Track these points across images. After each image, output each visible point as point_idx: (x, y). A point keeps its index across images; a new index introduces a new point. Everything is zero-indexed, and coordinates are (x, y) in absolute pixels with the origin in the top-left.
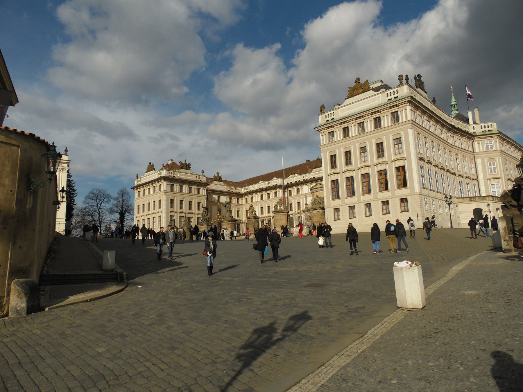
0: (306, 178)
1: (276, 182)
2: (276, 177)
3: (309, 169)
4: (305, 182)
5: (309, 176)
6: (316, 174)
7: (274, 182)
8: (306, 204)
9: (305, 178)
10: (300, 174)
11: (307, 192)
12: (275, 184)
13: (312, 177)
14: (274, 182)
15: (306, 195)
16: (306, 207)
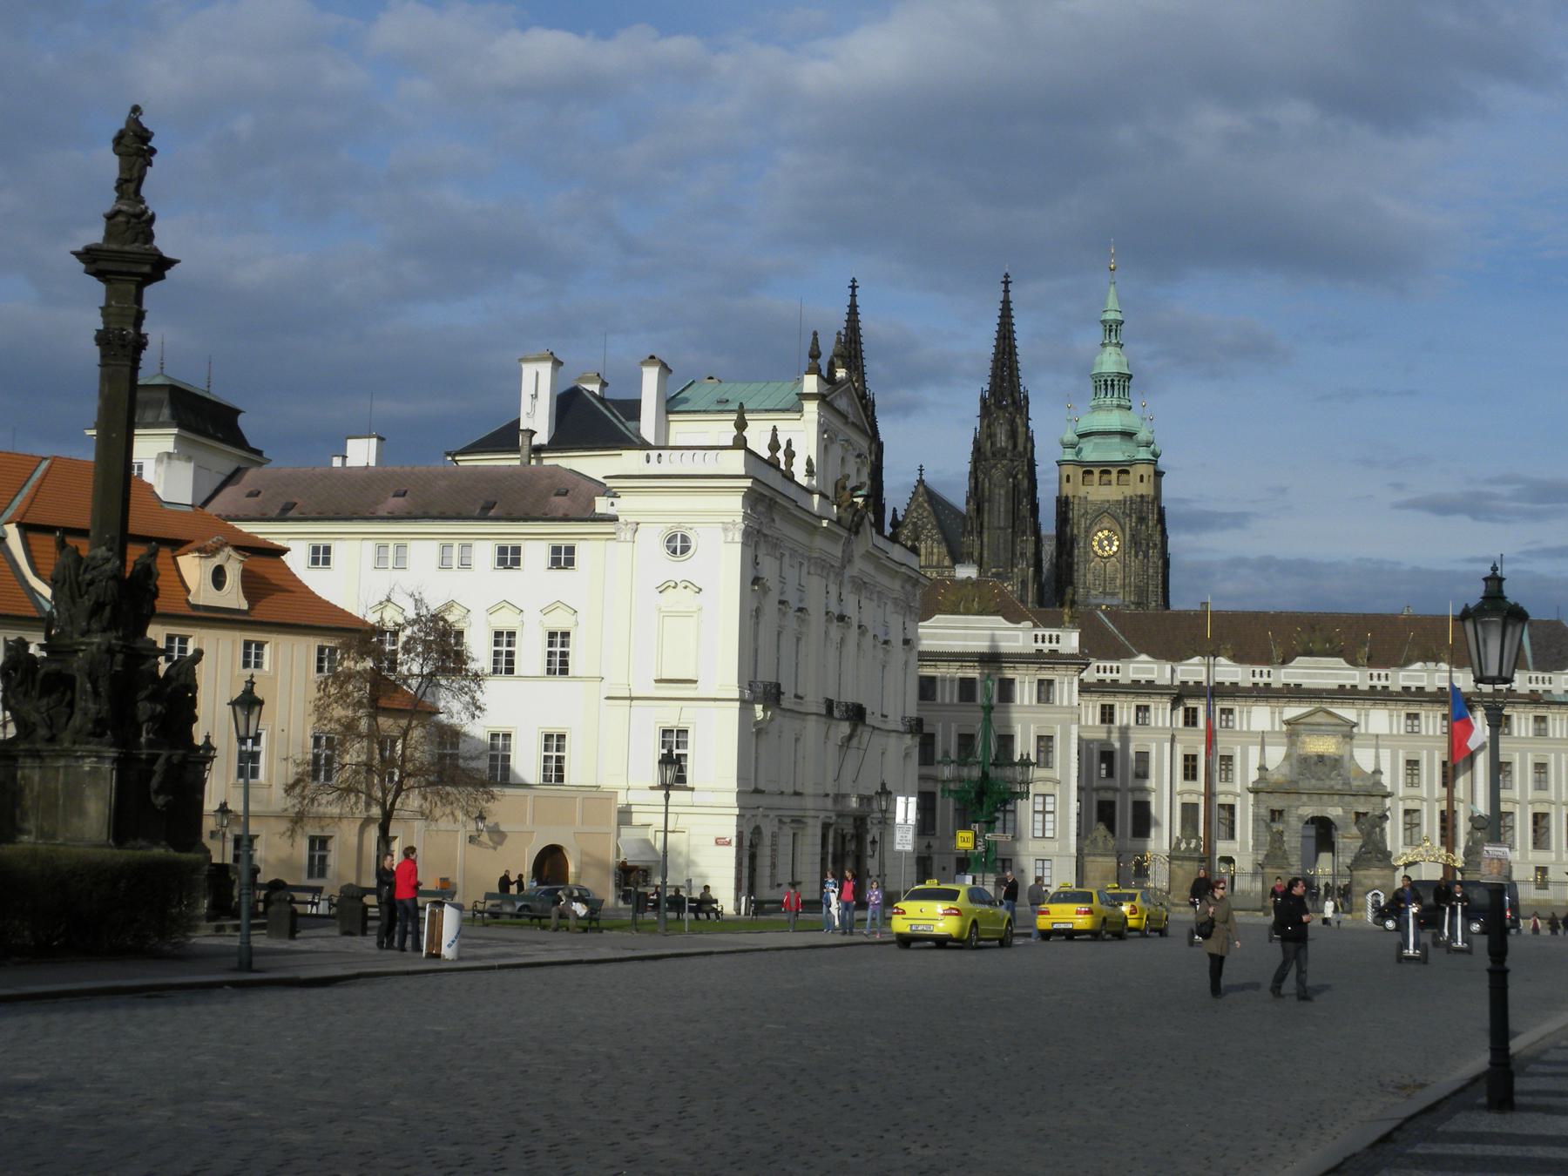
0: (1265, 679)
1: (1151, 671)
2: (1149, 655)
3: (1277, 652)
4: (1263, 693)
5: (1281, 676)
6: (1309, 676)
7: (1136, 671)
8: (1262, 768)
9: (1261, 681)
10: (1238, 658)
11: (1268, 728)
12: (1143, 677)
13: (1292, 681)
14: (1136, 671)
15: (1263, 739)
16: (1261, 779)
